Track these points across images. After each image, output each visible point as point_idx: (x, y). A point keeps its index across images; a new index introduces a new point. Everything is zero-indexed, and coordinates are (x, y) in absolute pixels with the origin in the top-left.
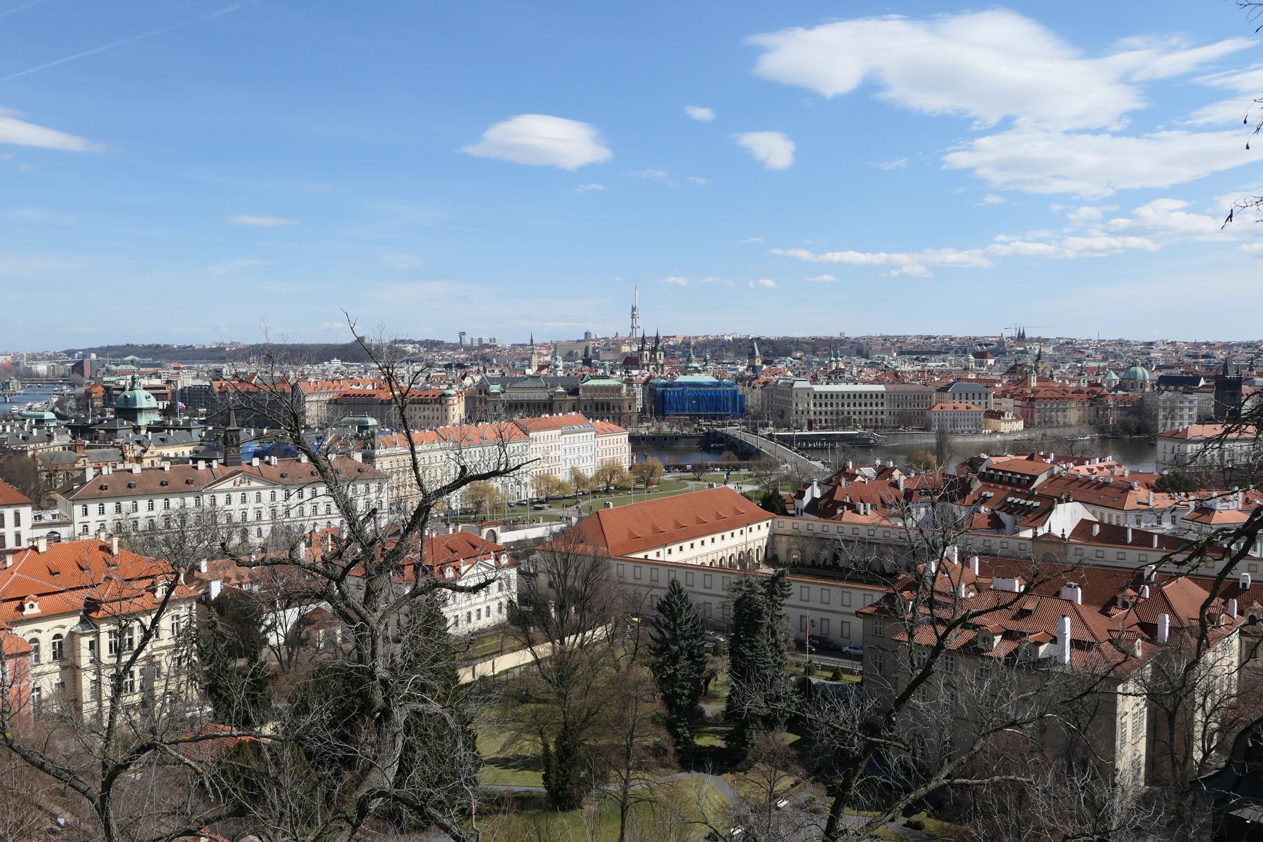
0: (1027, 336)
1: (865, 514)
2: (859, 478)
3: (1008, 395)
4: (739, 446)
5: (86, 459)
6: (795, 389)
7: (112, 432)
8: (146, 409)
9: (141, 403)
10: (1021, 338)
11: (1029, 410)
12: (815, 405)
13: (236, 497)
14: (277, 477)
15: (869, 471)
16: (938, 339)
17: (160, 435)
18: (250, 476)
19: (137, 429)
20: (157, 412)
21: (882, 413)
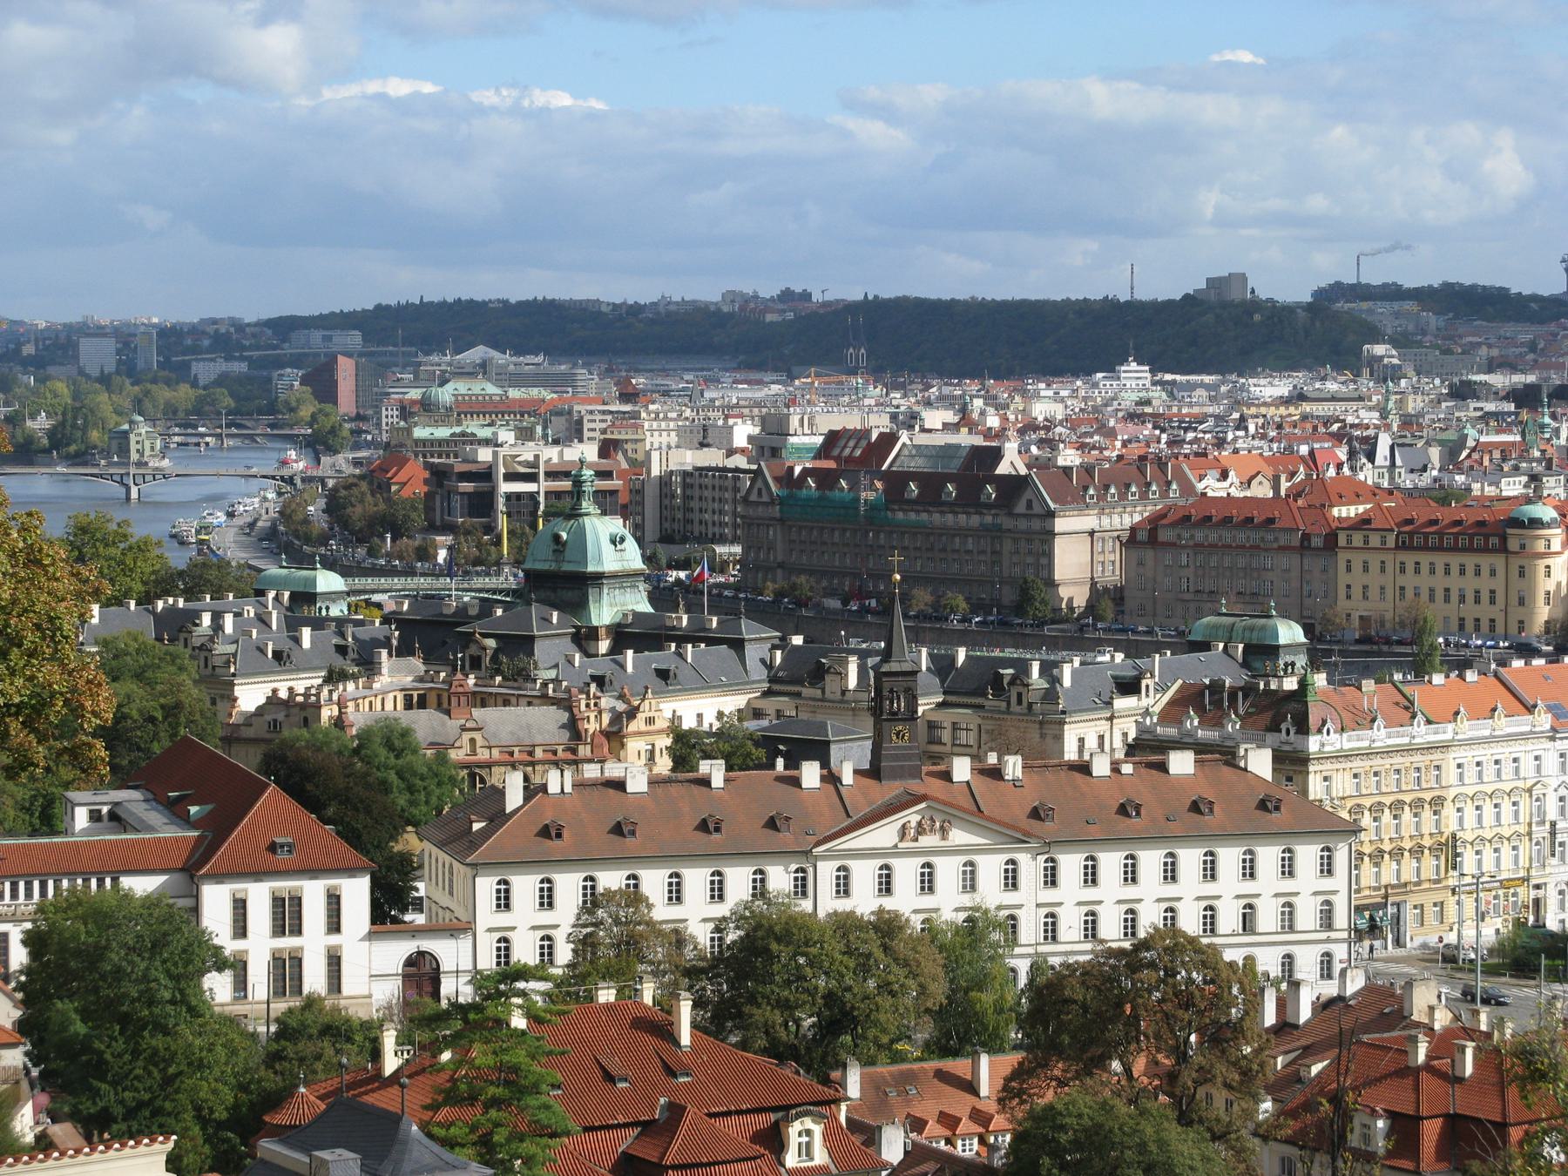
5: (477, 736)
7: (519, 645)
8: (614, 576)
9: (600, 561)
13: (906, 872)
14: (1020, 814)
17: (657, 659)
18: (949, 812)
19: (584, 638)
20: (642, 586)
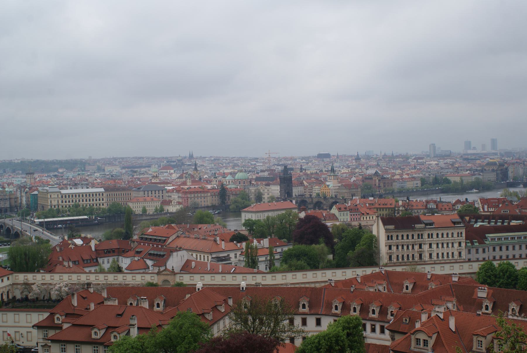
0: (194, 156)
1: (69, 266)
2: (71, 246)
3: (175, 191)
4: (11, 229)
6: (50, 193)
10: (191, 157)
11: (186, 199)
12: (62, 202)
15: (79, 242)
16: (145, 159)
21: (103, 205)
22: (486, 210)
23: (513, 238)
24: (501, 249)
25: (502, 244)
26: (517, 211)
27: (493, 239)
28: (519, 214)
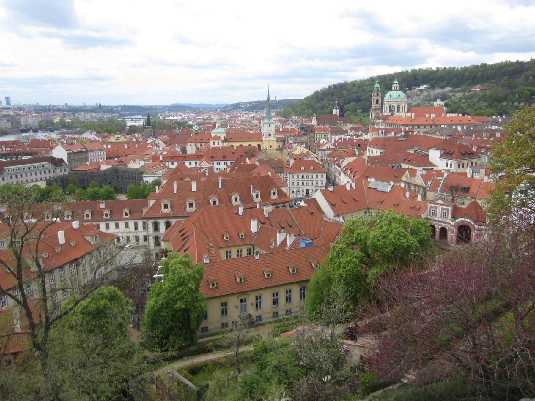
22: (4, 149)
23: (24, 169)
24: (16, 177)
25: (17, 173)
26: (28, 149)
27: (9, 171)
28: (30, 151)
